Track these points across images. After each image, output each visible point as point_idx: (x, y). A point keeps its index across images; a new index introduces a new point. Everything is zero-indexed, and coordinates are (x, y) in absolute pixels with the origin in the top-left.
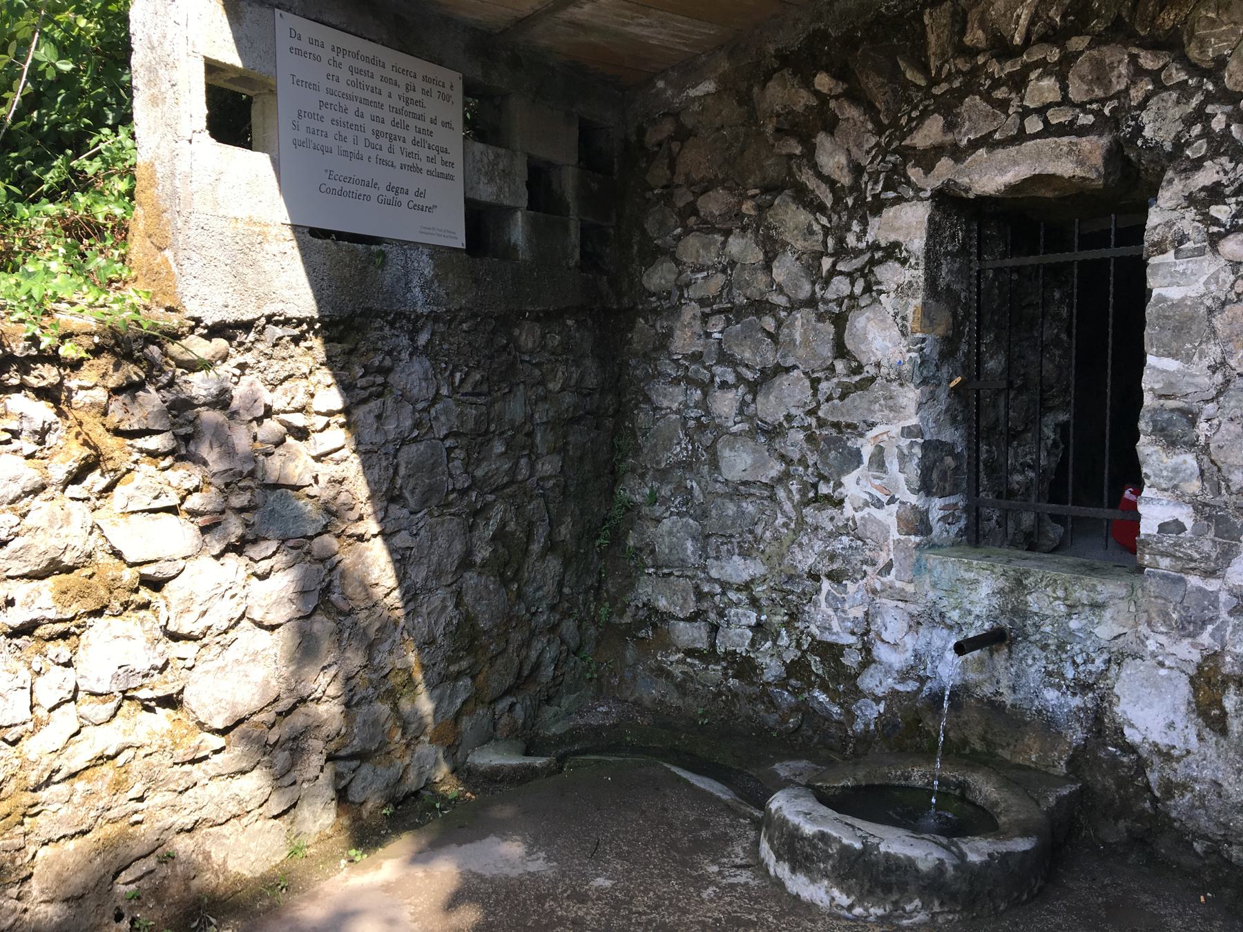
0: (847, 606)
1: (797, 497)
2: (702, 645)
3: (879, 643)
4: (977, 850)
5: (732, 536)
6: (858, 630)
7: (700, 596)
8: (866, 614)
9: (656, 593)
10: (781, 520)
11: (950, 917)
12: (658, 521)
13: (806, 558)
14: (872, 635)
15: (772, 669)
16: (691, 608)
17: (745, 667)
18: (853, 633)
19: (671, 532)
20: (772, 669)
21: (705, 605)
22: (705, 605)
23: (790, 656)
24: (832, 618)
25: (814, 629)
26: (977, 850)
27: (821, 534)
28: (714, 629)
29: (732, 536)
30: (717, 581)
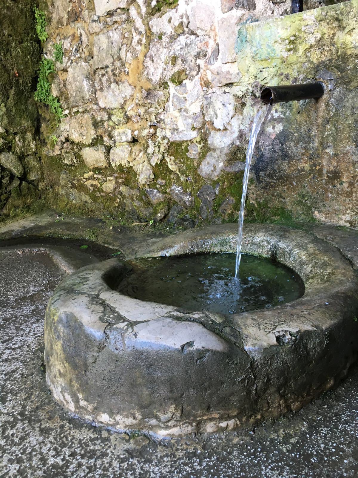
0: (187, 104)
1: (144, 9)
2: (103, 163)
3: (212, 132)
4: (259, 334)
5: (107, 67)
6: (197, 125)
7: (96, 124)
8: (202, 108)
9: (74, 129)
10: (136, 38)
11: (223, 424)
12: (65, 70)
13: (157, 71)
14: (207, 126)
15: (144, 175)
16: (92, 134)
17: (127, 175)
18: (194, 128)
19: (74, 77)
20: (144, 175)
21: (100, 131)
22: (100, 131)
23: (155, 160)
24: (179, 124)
25: (168, 134)
26: (259, 334)
27: (165, 39)
28: (108, 149)
29: (107, 67)
30: (104, 109)
